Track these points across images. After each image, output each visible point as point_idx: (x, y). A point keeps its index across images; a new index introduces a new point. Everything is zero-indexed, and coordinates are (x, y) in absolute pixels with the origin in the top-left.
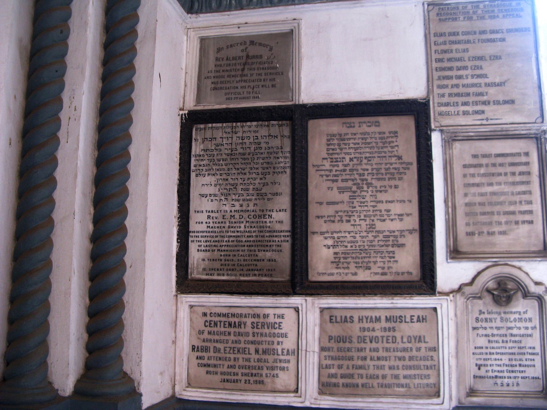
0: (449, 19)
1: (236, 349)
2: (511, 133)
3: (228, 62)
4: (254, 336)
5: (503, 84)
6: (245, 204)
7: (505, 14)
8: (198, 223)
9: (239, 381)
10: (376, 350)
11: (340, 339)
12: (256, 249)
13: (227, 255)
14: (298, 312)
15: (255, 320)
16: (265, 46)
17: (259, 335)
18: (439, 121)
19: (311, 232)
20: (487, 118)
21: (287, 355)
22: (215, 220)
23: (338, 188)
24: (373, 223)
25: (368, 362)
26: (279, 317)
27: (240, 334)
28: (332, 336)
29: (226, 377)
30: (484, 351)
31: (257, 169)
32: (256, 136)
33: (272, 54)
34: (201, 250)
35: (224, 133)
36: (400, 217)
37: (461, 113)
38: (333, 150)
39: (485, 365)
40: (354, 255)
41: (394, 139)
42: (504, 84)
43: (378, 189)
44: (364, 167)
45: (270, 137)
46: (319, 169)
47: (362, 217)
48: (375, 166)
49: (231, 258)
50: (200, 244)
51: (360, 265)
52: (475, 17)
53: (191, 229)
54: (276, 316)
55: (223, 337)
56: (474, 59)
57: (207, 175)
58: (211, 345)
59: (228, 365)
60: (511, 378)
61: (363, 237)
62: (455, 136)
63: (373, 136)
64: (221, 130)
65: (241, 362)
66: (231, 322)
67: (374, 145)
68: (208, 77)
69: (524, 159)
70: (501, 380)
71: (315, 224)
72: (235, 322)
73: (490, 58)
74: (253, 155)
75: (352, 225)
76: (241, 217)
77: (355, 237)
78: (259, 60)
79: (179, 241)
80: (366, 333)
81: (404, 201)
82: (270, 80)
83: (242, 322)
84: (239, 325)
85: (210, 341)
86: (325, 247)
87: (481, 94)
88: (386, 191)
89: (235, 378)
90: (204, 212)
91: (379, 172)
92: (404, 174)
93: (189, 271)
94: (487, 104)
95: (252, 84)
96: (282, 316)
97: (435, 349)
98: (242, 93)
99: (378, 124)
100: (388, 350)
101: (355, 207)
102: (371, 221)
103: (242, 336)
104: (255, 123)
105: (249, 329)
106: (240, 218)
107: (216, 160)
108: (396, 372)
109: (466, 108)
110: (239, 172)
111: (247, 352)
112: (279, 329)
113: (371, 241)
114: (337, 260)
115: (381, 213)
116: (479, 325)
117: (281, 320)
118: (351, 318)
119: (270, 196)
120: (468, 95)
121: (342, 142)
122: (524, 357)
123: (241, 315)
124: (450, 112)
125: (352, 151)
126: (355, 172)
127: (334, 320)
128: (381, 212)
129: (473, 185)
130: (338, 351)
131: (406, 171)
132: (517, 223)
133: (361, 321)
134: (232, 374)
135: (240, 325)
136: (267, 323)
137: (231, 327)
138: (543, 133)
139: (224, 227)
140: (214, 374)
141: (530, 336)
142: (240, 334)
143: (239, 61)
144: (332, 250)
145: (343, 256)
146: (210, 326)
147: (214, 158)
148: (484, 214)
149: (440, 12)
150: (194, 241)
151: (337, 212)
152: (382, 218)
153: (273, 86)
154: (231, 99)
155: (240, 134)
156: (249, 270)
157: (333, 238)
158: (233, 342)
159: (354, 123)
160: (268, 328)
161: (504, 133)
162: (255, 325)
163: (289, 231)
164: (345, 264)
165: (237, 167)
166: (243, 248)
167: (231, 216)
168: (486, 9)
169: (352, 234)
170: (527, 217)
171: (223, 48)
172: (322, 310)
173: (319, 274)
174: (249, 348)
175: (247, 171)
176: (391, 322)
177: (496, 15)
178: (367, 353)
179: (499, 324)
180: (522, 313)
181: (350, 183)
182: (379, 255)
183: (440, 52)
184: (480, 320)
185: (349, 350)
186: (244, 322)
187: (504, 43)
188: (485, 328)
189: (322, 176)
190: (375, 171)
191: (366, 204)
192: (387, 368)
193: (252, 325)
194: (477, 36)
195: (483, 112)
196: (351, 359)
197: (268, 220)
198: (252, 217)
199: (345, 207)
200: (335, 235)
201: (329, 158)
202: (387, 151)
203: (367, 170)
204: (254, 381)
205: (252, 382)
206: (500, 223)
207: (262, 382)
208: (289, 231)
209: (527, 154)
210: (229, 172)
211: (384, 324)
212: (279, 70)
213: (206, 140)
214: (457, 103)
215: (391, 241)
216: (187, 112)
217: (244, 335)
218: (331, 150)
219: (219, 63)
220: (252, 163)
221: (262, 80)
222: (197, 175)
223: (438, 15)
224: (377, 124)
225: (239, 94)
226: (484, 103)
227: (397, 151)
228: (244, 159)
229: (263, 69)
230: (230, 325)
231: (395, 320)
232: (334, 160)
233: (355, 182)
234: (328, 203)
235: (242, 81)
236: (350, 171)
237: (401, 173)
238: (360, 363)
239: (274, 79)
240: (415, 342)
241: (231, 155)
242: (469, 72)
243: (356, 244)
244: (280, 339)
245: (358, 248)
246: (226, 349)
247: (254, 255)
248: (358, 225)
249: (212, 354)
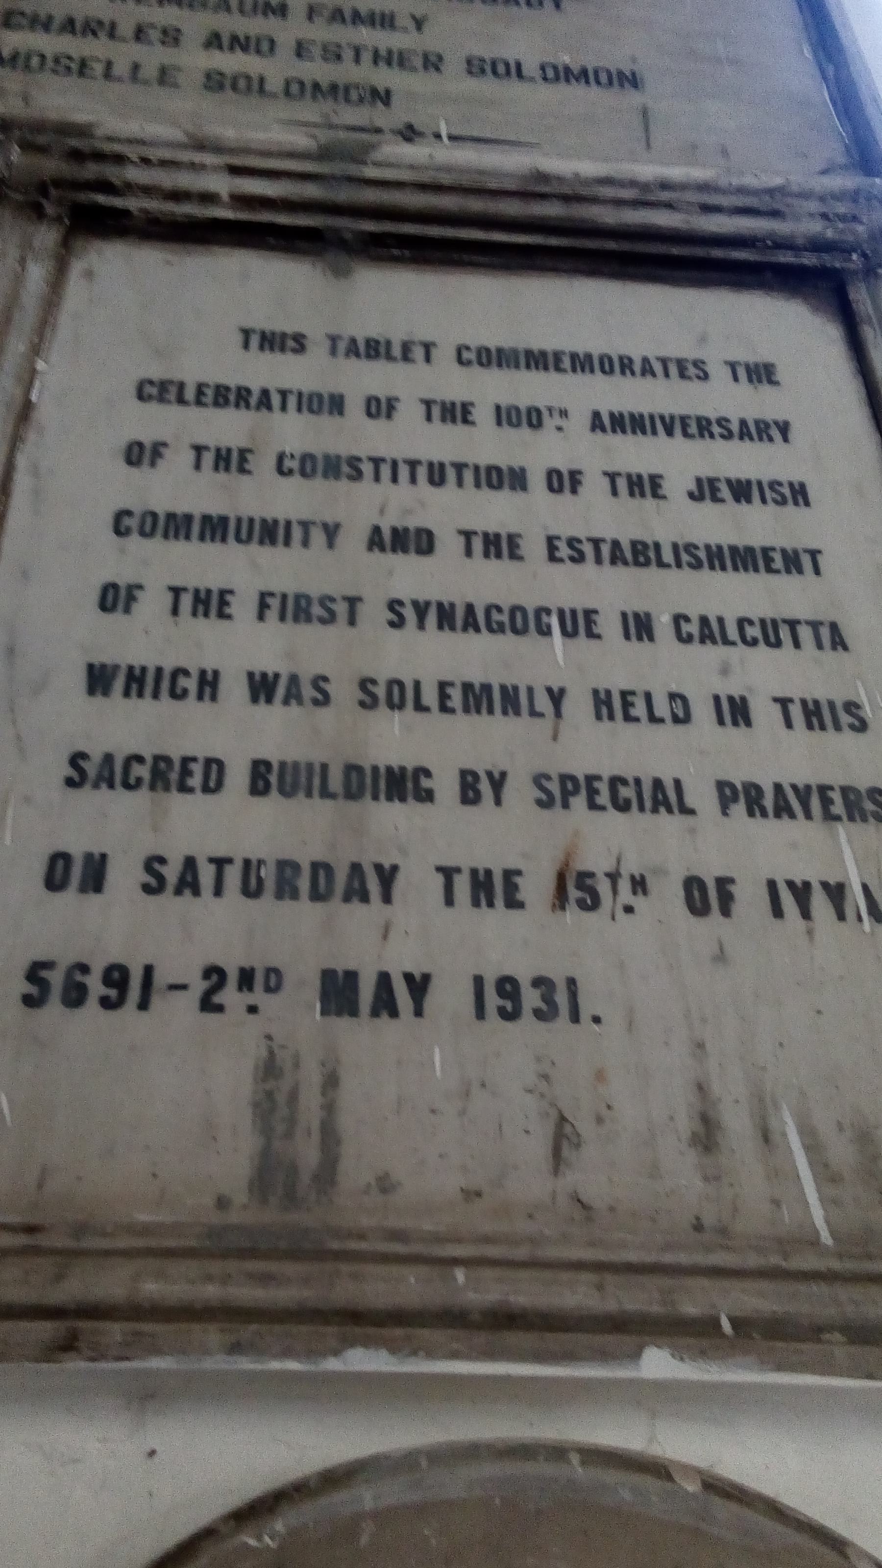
2: (608, 216)
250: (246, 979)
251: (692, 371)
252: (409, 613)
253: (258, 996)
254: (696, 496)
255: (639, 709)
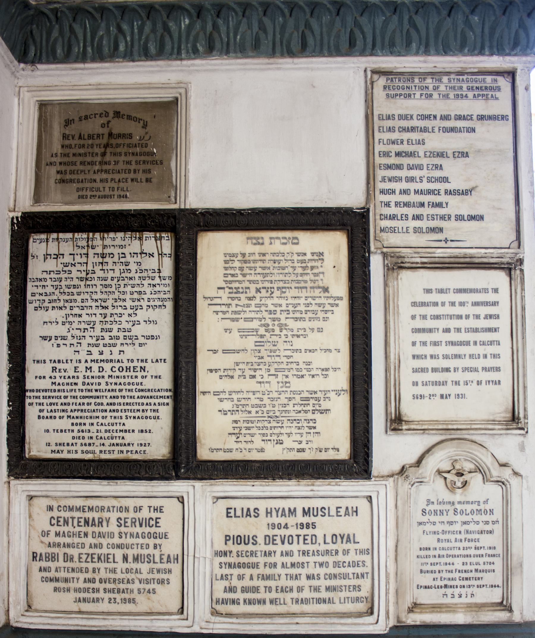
0: (401, 95)
1: (96, 557)
2: (477, 260)
3: (82, 142)
4: (121, 537)
5: (469, 192)
6: (106, 350)
7: (476, 93)
8: (38, 379)
9: (100, 601)
10: (288, 554)
11: (240, 540)
12: (124, 415)
13: (80, 424)
14: (183, 503)
15: (123, 515)
16: (137, 120)
17: (128, 535)
18: (381, 240)
19: (201, 392)
20: (446, 238)
21: (168, 562)
22: (63, 374)
23: (239, 330)
24: (287, 380)
25: (279, 570)
26: (155, 510)
27: (100, 535)
28: (229, 536)
29: (82, 595)
30: (431, 553)
31: (124, 300)
32: (122, 254)
33: (147, 133)
34: (43, 417)
35: (76, 248)
36: (324, 373)
37: (411, 230)
38: (233, 275)
40: (259, 425)
41: (319, 264)
42: (471, 192)
43: (295, 332)
44: (276, 301)
45: (143, 255)
46: (213, 302)
47: (272, 372)
48: (290, 301)
49: (87, 427)
50: (41, 407)
51: (269, 438)
52: (435, 95)
53: (29, 386)
54: (152, 509)
55: (76, 540)
56: (432, 155)
57: (50, 309)
58: (61, 551)
59: (85, 579)
60: (464, 587)
61: (272, 399)
62: (402, 263)
63: (289, 258)
64: (71, 243)
65: (103, 574)
66: (89, 518)
67: (290, 270)
68: (51, 164)
69: (491, 297)
70: (452, 590)
72: (94, 519)
73: (454, 155)
74: (118, 281)
75: (258, 382)
76: (101, 369)
77: (261, 400)
78: (127, 141)
79: (11, 403)
80: (276, 531)
81: (330, 351)
82: (144, 171)
83: (104, 519)
84: (99, 522)
85: (59, 545)
86: (220, 412)
87: (439, 205)
88: (305, 336)
89: (95, 595)
90: (48, 361)
91: (297, 309)
92: (331, 312)
93: (27, 446)
94: (447, 219)
95: (117, 177)
96: (160, 509)
97: (369, 551)
98: (102, 189)
100: (305, 553)
101: (262, 358)
102: (284, 377)
103: (104, 537)
105: (113, 527)
106: (99, 371)
107: (64, 287)
108: (315, 583)
109: (417, 224)
110: (98, 304)
111: (111, 560)
112: (156, 526)
113: (285, 405)
114: (236, 431)
115: (297, 367)
116: (425, 519)
117: (158, 515)
118: (256, 511)
119: (142, 340)
120: (422, 205)
121: (245, 265)
122: (481, 560)
123: (102, 509)
124: (396, 229)
125: (259, 278)
126: (263, 308)
127: (232, 514)
128: (298, 365)
129: (423, 330)
130: (238, 556)
131: (334, 308)
132: (479, 383)
133: (269, 515)
134: (91, 590)
135: (101, 523)
136: (139, 519)
137: (88, 526)
138: (518, 263)
139: (76, 384)
140: (64, 592)
142: (100, 535)
143: (98, 142)
144: (230, 418)
145: (246, 425)
146: (58, 525)
147: (61, 284)
149: (387, 85)
150: (32, 403)
151: (237, 364)
152: (300, 373)
153: (148, 180)
154: (86, 198)
155: (99, 250)
156: (113, 445)
157: (232, 400)
158: (91, 547)
159: (262, 238)
160: (141, 525)
161: (468, 260)
162: (122, 522)
163: (170, 390)
164: (248, 436)
165: (95, 297)
166: (104, 414)
167: (86, 367)
168: (451, 85)
169: (258, 395)
171: (73, 120)
173: (212, 450)
174: (114, 555)
175: (109, 303)
176: (310, 516)
177: (464, 94)
178: (278, 559)
179: (451, 517)
180: (481, 503)
181: (255, 324)
182: (295, 424)
183: (385, 142)
184: (427, 512)
185: (253, 554)
186: (106, 518)
187: (472, 134)
188: (434, 523)
189: (217, 312)
190: (291, 308)
191: (277, 353)
192: (304, 577)
193: (118, 521)
194: (438, 123)
195: (441, 230)
196: (255, 566)
197: (139, 374)
198: (117, 369)
200: (235, 396)
201: (227, 287)
202: (308, 280)
203: (280, 305)
204: (122, 599)
205: (118, 600)
206: (457, 383)
208: (170, 390)
209: (496, 291)
210: (83, 304)
211: (300, 518)
212: (157, 158)
213: (49, 257)
214: (407, 216)
215: (311, 405)
216: (20, 214)
217: (106, 537)
218: (229, 276)
219: (67, 142)
220: (116, 292)
221: (132, 172)
222: (36, 309)
223: (385, 87)
224: (296, 241)
225: (98, 190)
226: (442, 218)
227: (322, 280)
228: (106, 286)
229: (133, 154)
230: (87, 522)
231: (315, 513)
232: (235, 290)
233: (263, 322)
234: (225, 351)
235: (102, 171)
236: (256, 307)
237: (326, 312)
238: (268, 571)
239: (149, 171)
240: (342, 542)
241: (87, 279)
242: (424, 173)
243: (262, 409)
244: (158, 541)
245: (265, 414)
246: (81, 556)
247: (120, 423)
248: (267, 382)
249: (61, 563)
250: (433, 395)
251: (487, 291)
252: (448, 343)
253: (434, 397)
254: (484, 318)
255: (474, 357)
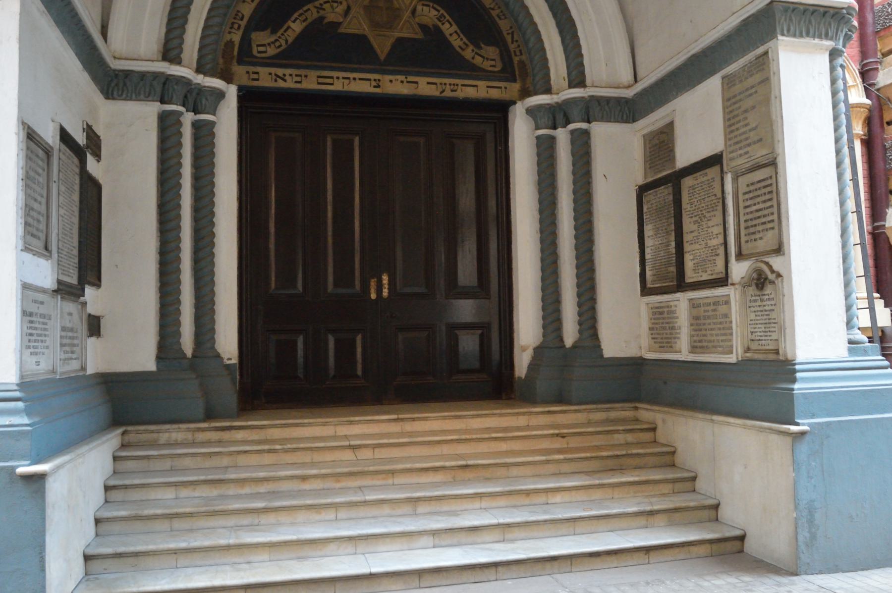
2: (761, 164)
39: (755, 332)
69: (769, 182)
71: (687, 247)
87: (747, 139)
99: (706, 174)
104: (663, 187)
141: (773, 310)
144: (693, 262)
148: (752, 226)
151: (693, 237)
170: (771, 225)
172: (690, 300)
179: (759, 303)
199: (695, 234)
207: (671, 347)
244: (676, 320)
